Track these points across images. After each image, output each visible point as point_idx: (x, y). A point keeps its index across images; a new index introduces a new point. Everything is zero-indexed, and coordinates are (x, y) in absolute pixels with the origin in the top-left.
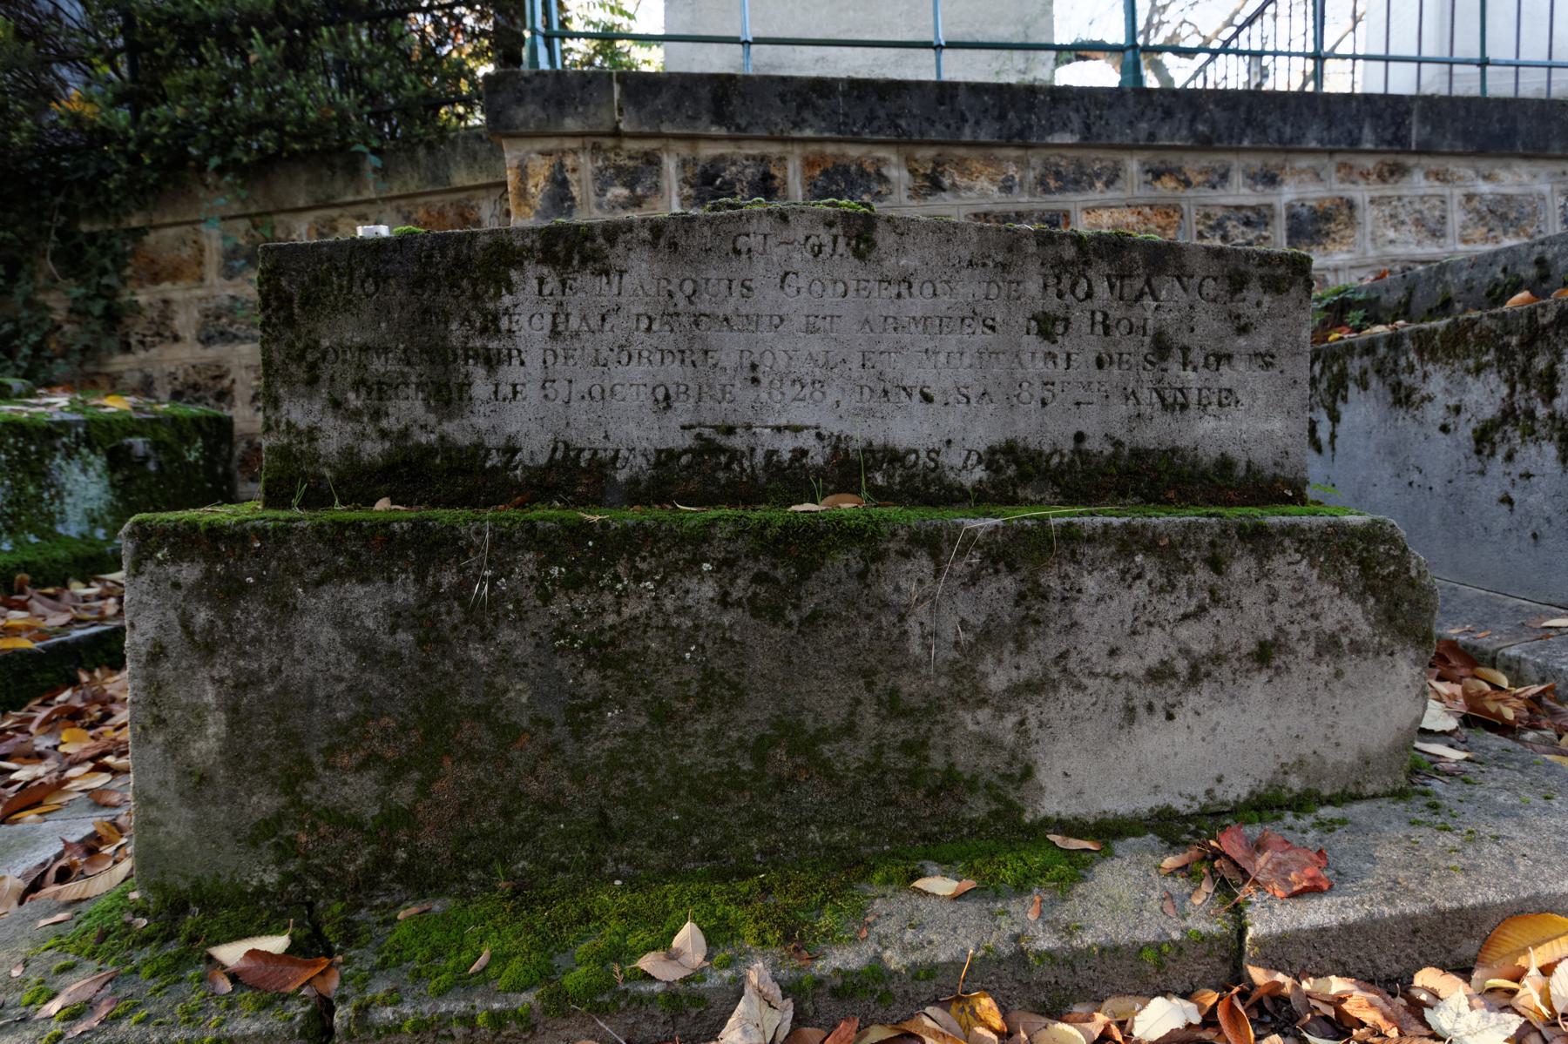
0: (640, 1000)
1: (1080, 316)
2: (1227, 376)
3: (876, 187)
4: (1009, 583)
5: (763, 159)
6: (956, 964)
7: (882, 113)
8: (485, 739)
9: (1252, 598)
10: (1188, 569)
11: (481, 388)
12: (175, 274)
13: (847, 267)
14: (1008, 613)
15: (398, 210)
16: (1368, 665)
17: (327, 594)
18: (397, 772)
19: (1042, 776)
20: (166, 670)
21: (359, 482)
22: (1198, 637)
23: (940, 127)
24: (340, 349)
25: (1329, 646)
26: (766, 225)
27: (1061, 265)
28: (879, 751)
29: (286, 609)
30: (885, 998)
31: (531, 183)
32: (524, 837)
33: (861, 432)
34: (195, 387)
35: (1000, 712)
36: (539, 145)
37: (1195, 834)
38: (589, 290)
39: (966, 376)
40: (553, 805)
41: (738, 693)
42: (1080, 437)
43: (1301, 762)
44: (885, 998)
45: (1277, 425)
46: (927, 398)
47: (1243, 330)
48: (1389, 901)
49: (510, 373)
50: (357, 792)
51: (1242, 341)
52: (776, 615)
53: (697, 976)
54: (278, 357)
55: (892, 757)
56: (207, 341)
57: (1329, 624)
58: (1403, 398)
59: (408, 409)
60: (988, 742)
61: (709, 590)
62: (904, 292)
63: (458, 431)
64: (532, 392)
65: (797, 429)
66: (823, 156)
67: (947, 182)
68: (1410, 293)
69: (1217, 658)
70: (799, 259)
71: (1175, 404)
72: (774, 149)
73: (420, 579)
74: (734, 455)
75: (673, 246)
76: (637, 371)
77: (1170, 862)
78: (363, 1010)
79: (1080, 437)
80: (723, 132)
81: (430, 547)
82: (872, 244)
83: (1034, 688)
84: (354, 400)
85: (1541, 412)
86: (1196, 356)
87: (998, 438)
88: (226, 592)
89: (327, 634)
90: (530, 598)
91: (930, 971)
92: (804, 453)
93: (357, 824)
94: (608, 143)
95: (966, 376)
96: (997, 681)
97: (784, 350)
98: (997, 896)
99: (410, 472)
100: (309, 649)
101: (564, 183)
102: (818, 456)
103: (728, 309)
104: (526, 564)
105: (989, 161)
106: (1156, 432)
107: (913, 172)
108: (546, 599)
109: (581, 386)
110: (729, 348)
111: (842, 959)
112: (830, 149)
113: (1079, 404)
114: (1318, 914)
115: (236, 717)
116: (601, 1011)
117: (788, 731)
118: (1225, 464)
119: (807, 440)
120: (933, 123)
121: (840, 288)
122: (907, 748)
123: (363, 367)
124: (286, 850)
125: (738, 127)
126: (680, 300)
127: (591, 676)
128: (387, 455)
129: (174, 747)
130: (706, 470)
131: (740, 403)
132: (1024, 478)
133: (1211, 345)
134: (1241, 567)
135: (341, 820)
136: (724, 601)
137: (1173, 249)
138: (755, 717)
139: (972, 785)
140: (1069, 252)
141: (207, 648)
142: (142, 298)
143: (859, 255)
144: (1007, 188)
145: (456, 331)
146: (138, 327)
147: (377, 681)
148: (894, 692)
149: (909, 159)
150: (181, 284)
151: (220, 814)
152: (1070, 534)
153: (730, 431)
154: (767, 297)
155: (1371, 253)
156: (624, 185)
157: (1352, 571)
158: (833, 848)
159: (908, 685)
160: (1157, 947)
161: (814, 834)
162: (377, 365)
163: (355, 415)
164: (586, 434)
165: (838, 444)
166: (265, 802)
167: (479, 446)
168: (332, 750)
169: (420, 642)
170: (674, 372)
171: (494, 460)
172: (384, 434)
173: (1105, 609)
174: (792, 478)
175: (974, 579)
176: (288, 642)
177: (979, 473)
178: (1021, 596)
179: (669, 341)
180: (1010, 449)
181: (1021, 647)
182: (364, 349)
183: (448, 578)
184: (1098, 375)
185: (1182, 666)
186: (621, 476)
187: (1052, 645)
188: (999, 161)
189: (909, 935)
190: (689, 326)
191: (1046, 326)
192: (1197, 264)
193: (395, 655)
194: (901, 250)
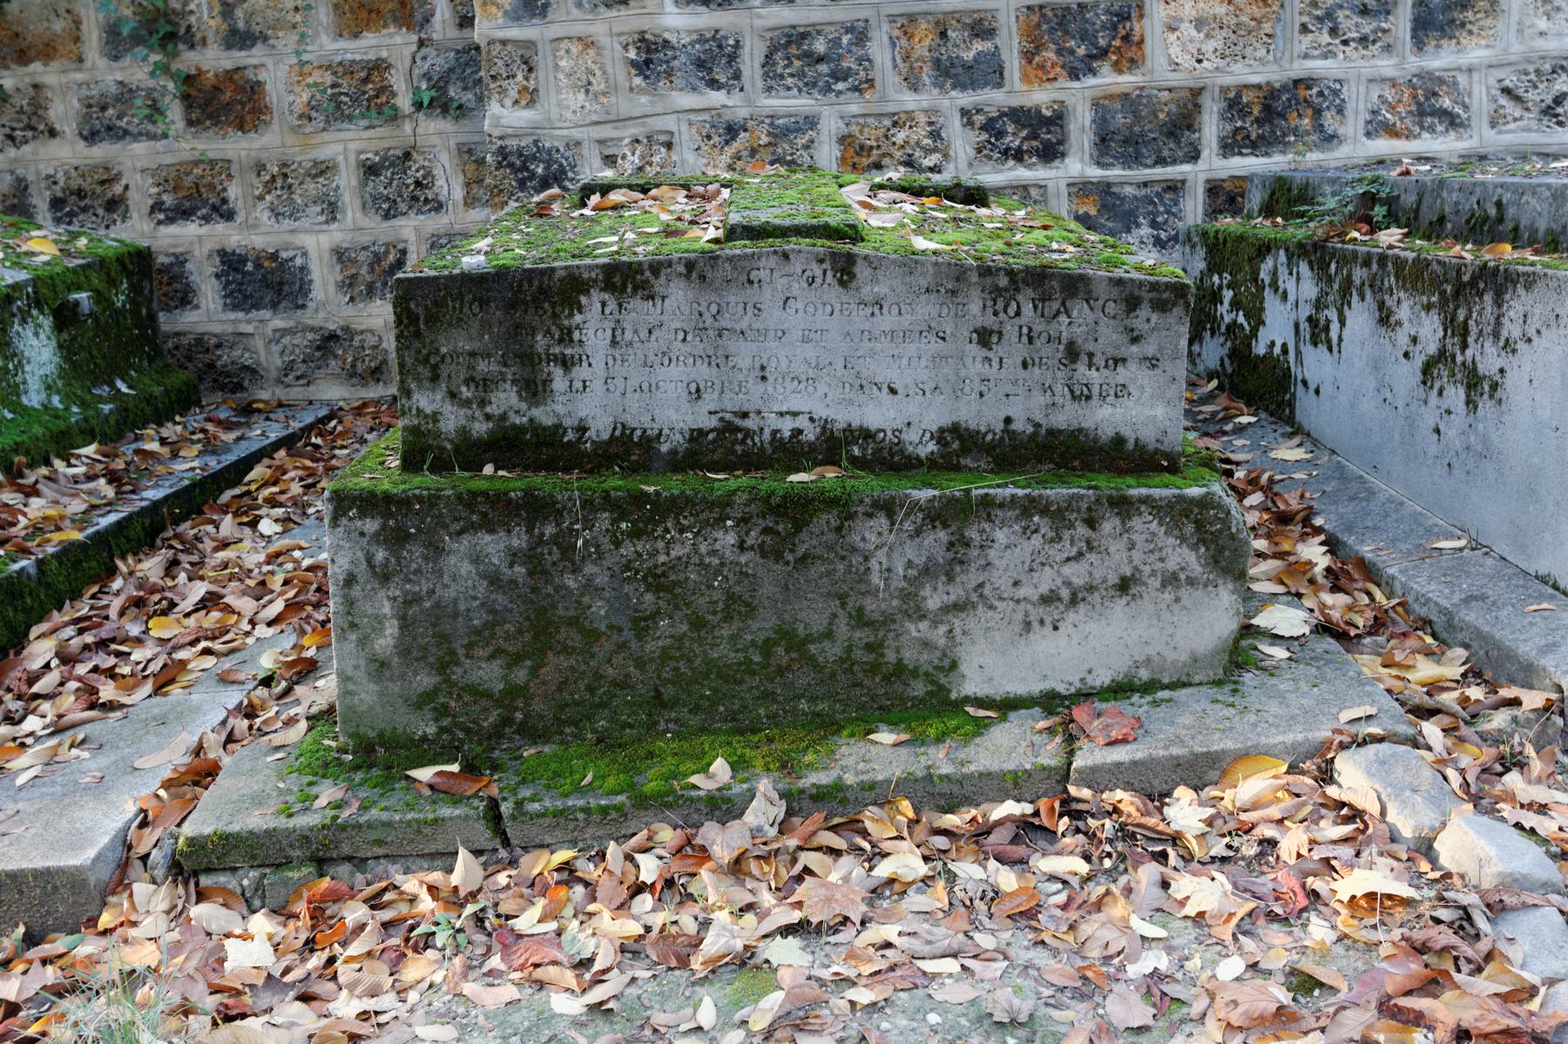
0: (691, 800)
1: (1010, 330)
4: (943, 535)
6: (888, 782)
8: (575, 639)
9: (1117, 548)
10: (1071, 526)
11: (559, 383)
12: (47, 52)
13: (833, 293)
14: (941, 556)
16: (1199, 593)
17: (466, 540)
18: (515, 660)
19: (964, 668)
20: (356, 591)
21: (470, 453)
22: (1077, 573)
24: (454, 355)
26: (773, 262)
27: (997, 291)
28: (849, 649)
29: (436, 550)
30: (844, 802)
32: (603, 705)
33: (842, 417)
34: (80, 193)
35: (935, 624)
38: (639, 311)
39: (923, 375)
40: (623, 684)
41: (751, 610)
42: (1008, 420)
43: (1148, 660)
44: (844, 802)
45: (1160, 411)
46: (893, 391)
47: (1135, 340)
48: (1166, 747)
49: (580, 372)
50: (489, 674)
51: (1134, 349)
52: (778, 556)
53: (727, 787)
54: (409, 361)
55: (858, 654)
56: (91, 137)
57: (1172, 565)
58: (1385, 319)
59: (506, 399)
60: (926, 644)
61: (731, 539)
62: (877, 311)
63: (543, 415)
64: (597, 386)
65: (795, 414)
68: (1419, 202)
69: (1091, 588)
70: (798, 287)
71: (1081, 396)
73: (530, 531)
74: (748, 433)
75: (702, 278)
76: (675, 371)
77: (1042, 724)
78: (519, 804)
79: (1008, 420)
81: (535, 508)
82: (852, 276)
83: (958, 607)
84: (466, 393)
85: (1459, 359)
86: (1099, 360)
87: (946, 421)
88: (396, 539)
89: (466, 568)
90: (607, 545)
91: (872, 786)
92: (800, 432)
93: (488, 695)
95: (923, 375)
96: (933, 602)
98: (923, 743)
99: (509, 445)
100: (454, 578)
102: (810, 434)
103: (744, 325)
104: (604, 520)
106: (1067, 416)
108: (617, 544)
109: (633, 383)
110: (745, 354)
113: (1009, 397)
114: (1121, 754)
115: (405, 623)
116: (669, 806)
117: (785, 635)
118: (1119, 440)
119: (802, 422)
121: (828, 309)
122: (869, 647)
123: (471, 368)
124: (442, 712)
126: (707, 316)
127: (649, 597)
128: (491, 432)
129: (363, 642)
130: (726, 446)
131: (752, 395)
132: (965, 450)
133: (1110, 352)
134: (1109, 525)
135: (478, 692)
136: (741, 547)
137: (1084, 279)
138: (763, 625)
139: (915, 673)
140: (1003, 281)
141: (384, 576)
143: (842, 283)
145: (541, 341)
147: (501, 599)
148: (860, 610)
150: (55, 65)
151: (395, 688)
152: (987, 502)
153: (745, 415)
154: (773, 316)
155: (1516, 48)
157: (1190, 528)
158: (818, 715)
159: (870, 605)
160: (1015, 773)
161: (803, 705)
162: (483, 366)
163: (467, 403)
164: (639, 418)
165: (825, 426)
166: (425, 680)
167: (558, 426)
168: (469, 646)
169: (531, 574)
170: (703, 372)
171: (570, 436)
172: (488, 417)
173: (1009, 552)
174: (791, 452)
175: (918, 532)
176: (439, 573)
177: (932, 447)
178: (952, 544)
179: (699, 348)
180: (955, 429)
181: (951, 579)
182: (472, 354)
183: (549, 530)
184: (1022, 374)
185: (1065, 593)
186: (664, 448)
187: (973, 577)
189: (861, 766)
190: (712, 335)
191: (984, 337)
192: (1101, 290)
193: (513, 582)
194: (875, 281)
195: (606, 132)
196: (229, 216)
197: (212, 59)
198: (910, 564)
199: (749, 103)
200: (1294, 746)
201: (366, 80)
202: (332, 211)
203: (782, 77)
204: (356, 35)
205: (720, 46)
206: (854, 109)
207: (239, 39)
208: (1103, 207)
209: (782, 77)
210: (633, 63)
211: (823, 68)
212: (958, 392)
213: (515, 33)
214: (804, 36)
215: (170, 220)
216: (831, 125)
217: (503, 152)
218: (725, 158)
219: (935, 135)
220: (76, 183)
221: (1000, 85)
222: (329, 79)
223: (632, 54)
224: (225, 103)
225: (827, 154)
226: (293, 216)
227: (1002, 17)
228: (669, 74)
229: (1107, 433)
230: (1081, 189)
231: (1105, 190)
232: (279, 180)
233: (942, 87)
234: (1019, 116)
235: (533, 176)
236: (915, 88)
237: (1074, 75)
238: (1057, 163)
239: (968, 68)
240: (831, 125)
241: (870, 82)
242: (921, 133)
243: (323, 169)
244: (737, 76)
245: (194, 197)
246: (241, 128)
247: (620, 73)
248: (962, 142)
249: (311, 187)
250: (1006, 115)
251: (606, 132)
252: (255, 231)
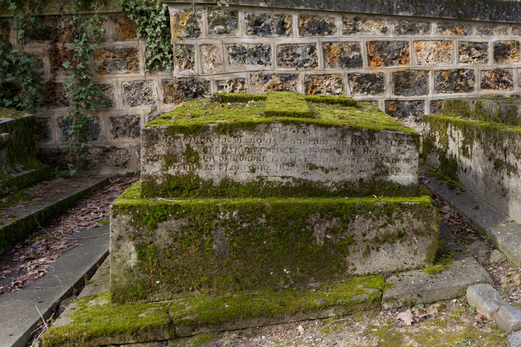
62: (316, 143)
92: (289, 183)
121: (299, 141)
144: (384, 31)
203: (285, 61)
205: (263, 50)
206: (309, 73)
209: (285, 61)
218: (264, 88)
223: (231, 51)
233: (342, 66)
234: (368, 77)
238: (381, 94)
250: (364, 76)
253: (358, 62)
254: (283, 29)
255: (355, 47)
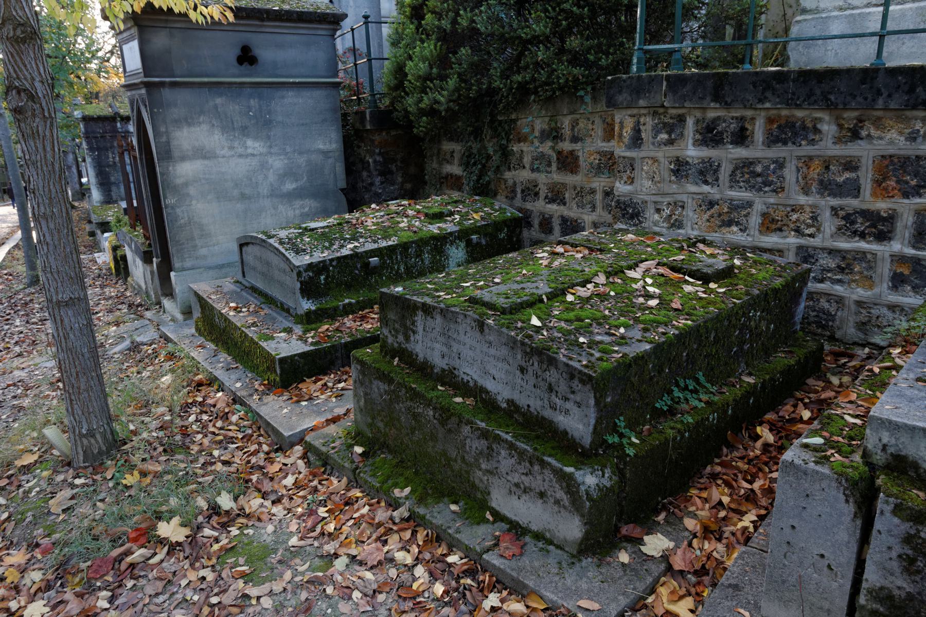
2: (568, 405)
3: (811, 136)
5: (742, 119)
7: (818, 92)
15: (601, 117)
16: (567, 514)
22: (526, 480)
23: (860, 99)
25: (557, 502)
27: (526, 353)
31: (624, 131)
35: (484, 475)
36: (629, 112)
37: (517, 530)
42: (528, 406)
45: (581, 427)
46: (494, 378)
47: (573, 392)
49: (416, 336)
51: (572, 396)
55: (463, 472)
56: (533, 170)
59: (401, 338)
66: (780, 116)
67: (864, 133)
70: (469, 329)
72: (749, 113)
74: (456, 376)
80: (718, 106)
87: (510, 397)
94: (661, 110)
97: (467, 353)
101: (639, 131)
105: (900, 119)
106: (548, 413)
107: (841, 126)
111: (421, 511)
112: (785, 113)
118: (565, 433)
120: (854, 97)
125: (726, 103)
140: (528, 350)
142: (515, 149)
146: (514, 160)
149: (838, 118)
156: (667, 133)
157: (564, 484)
184: (534, 390)
188: (908, 119)
191: (523, 370)
192: (561, 366)
194: (489, 334)
195: (658, 199)
196: (565, 204)
197: (566, 146)
198: (477, 448)
199: (721, 192)
200: (552, 601)
201: (610, 159)
202: (594, 208)
203: (738, 182)
204: (609, 141)
205: (711, 166)
206: (772, 200)
207: (575, 139)
208: (914, 271)
209: (738, 182)
210: (672, 170)
211: (759, 179)
212: (513, 388)
213: (628, 154)
214: (751, 163)
215: (549, 203)
216: (759, 207)
217: (618, 202)
218: (706, 216)
219: (814, 218)
220: (528, 185)
221: (857, 197)
222: (598, 157)
223: (672, 167)
224: (568, 162)
225: (755, 220)
226: (583, 207)
227: (864, 161)
228: (687, 176)
229: (562, 427)
230: (899, 259)
231: (916, 262)
232: (581, 192)
233: (822, 194)
234: (866, 214)
235: (628, 213)
236: (806, 191)
237: (906, 195)
238: (885, 243)
239: (839, 186)
240: (759, 207)
241: (783, 189)
242: (806, 217)
243: (593, 192)
244: (717, 180)
245: (556, 196)
246: (572, 172)
247: (666, 174)
248: (829, 224)
249: (589, 198)
250: (858, 213)
251: (658, 199)
252: (571, 211)
253: (854, 189)
254: (741, 137)
255: (851, 165)
